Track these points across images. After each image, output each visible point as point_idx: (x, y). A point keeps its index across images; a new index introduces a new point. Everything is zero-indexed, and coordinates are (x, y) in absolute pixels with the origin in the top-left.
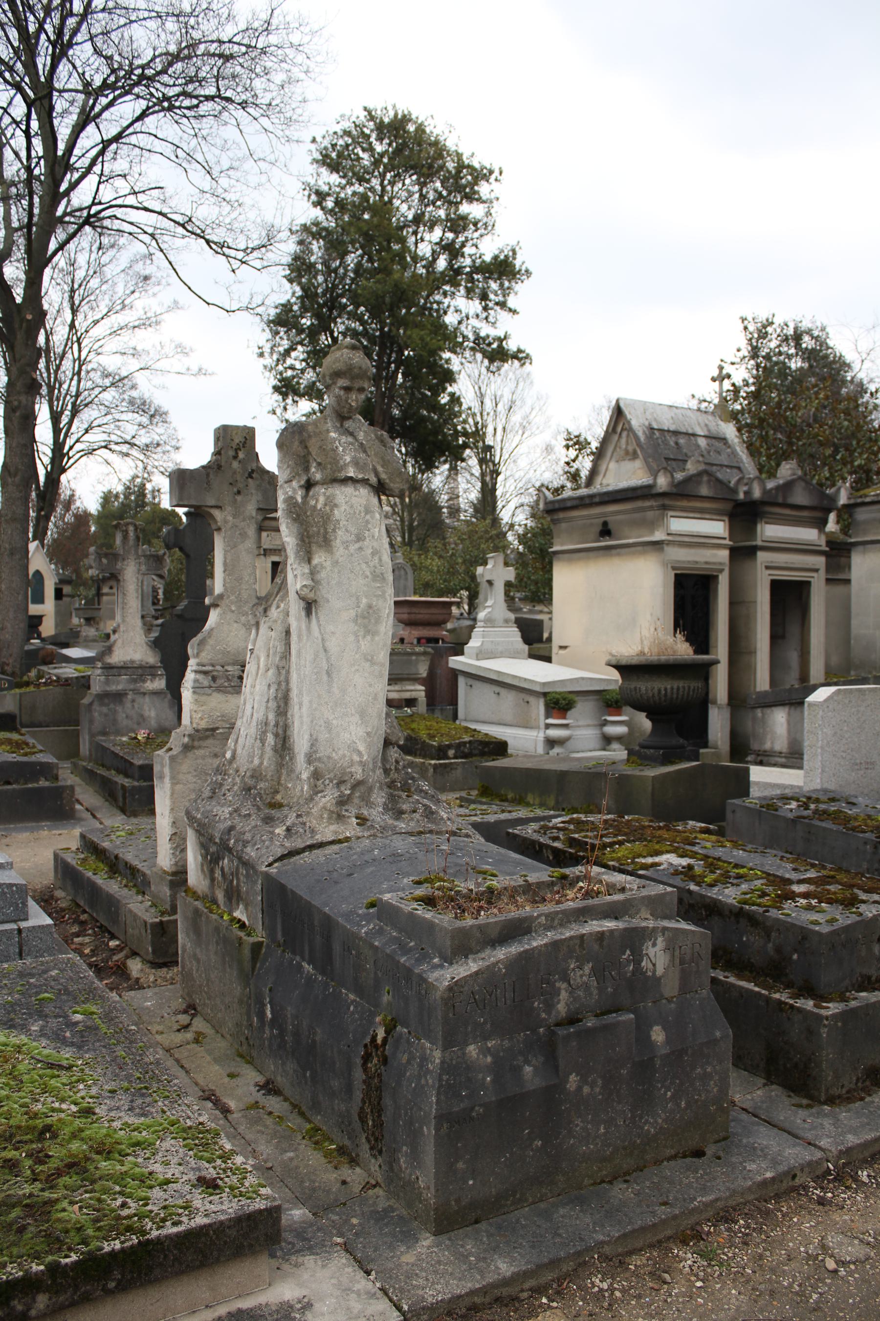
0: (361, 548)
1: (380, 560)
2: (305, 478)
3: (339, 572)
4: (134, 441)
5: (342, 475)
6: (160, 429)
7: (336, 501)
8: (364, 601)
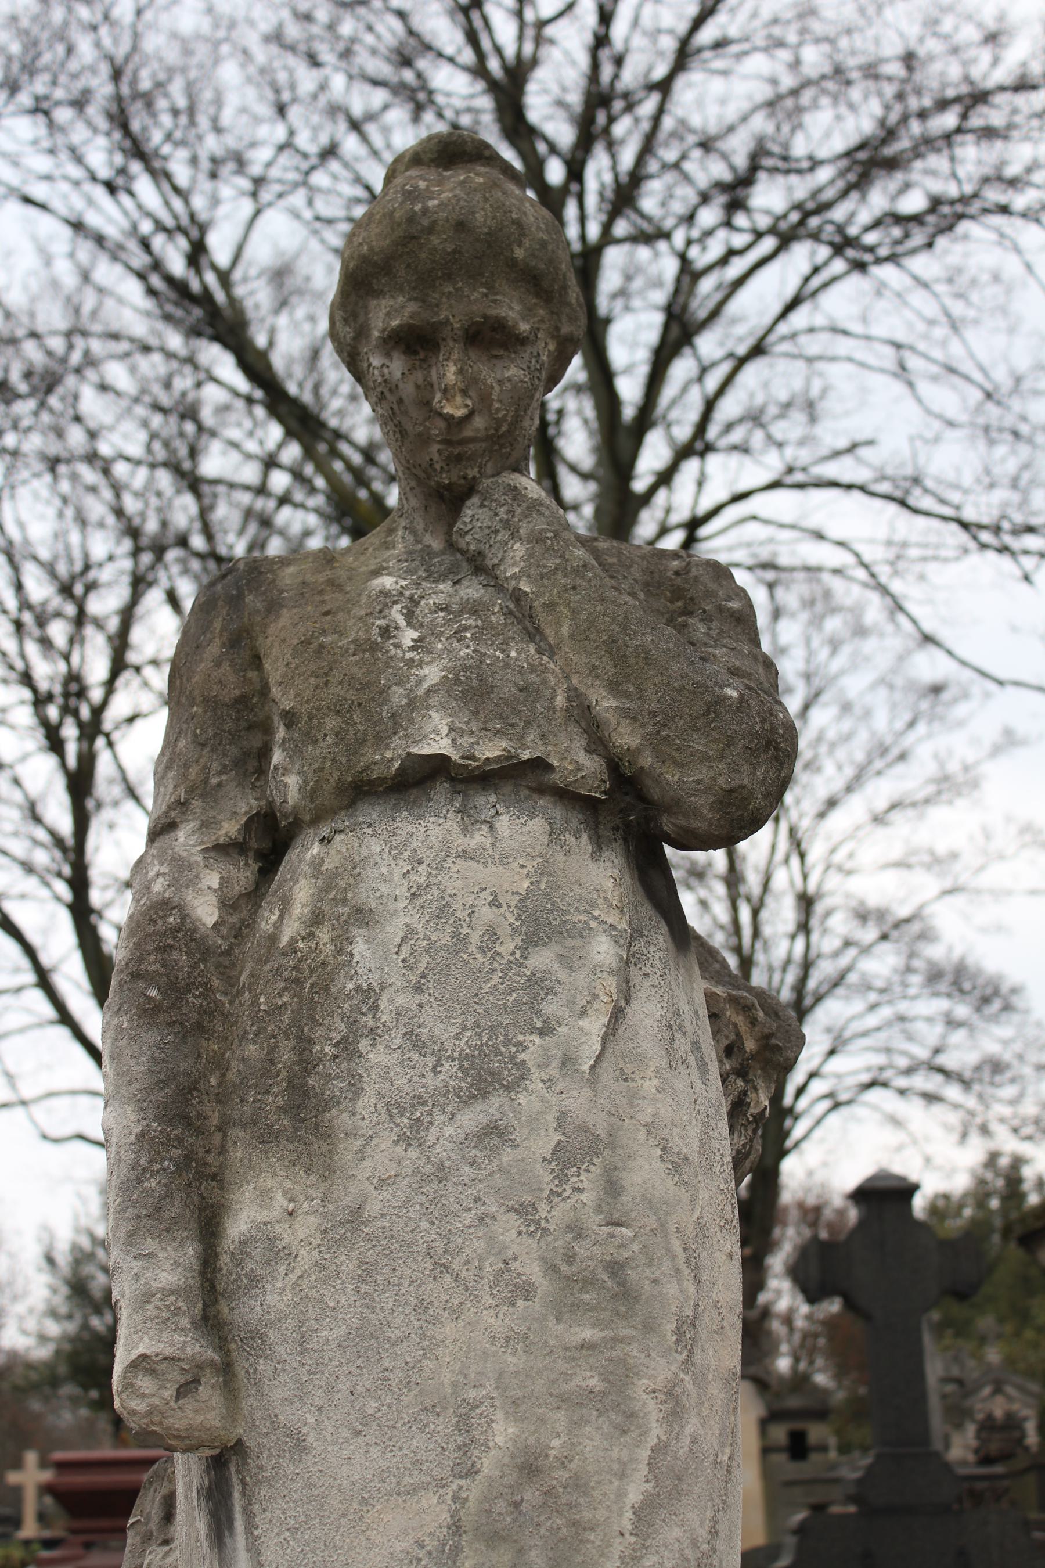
0: (494, 1133)
1: (612, 1187)
2: (246, 804)
3: (366, 1272)
4: (942, 1060)
5: (392, 755)
6: (1004, 1031)
7: (363, 895)
8: (503, 1433)
